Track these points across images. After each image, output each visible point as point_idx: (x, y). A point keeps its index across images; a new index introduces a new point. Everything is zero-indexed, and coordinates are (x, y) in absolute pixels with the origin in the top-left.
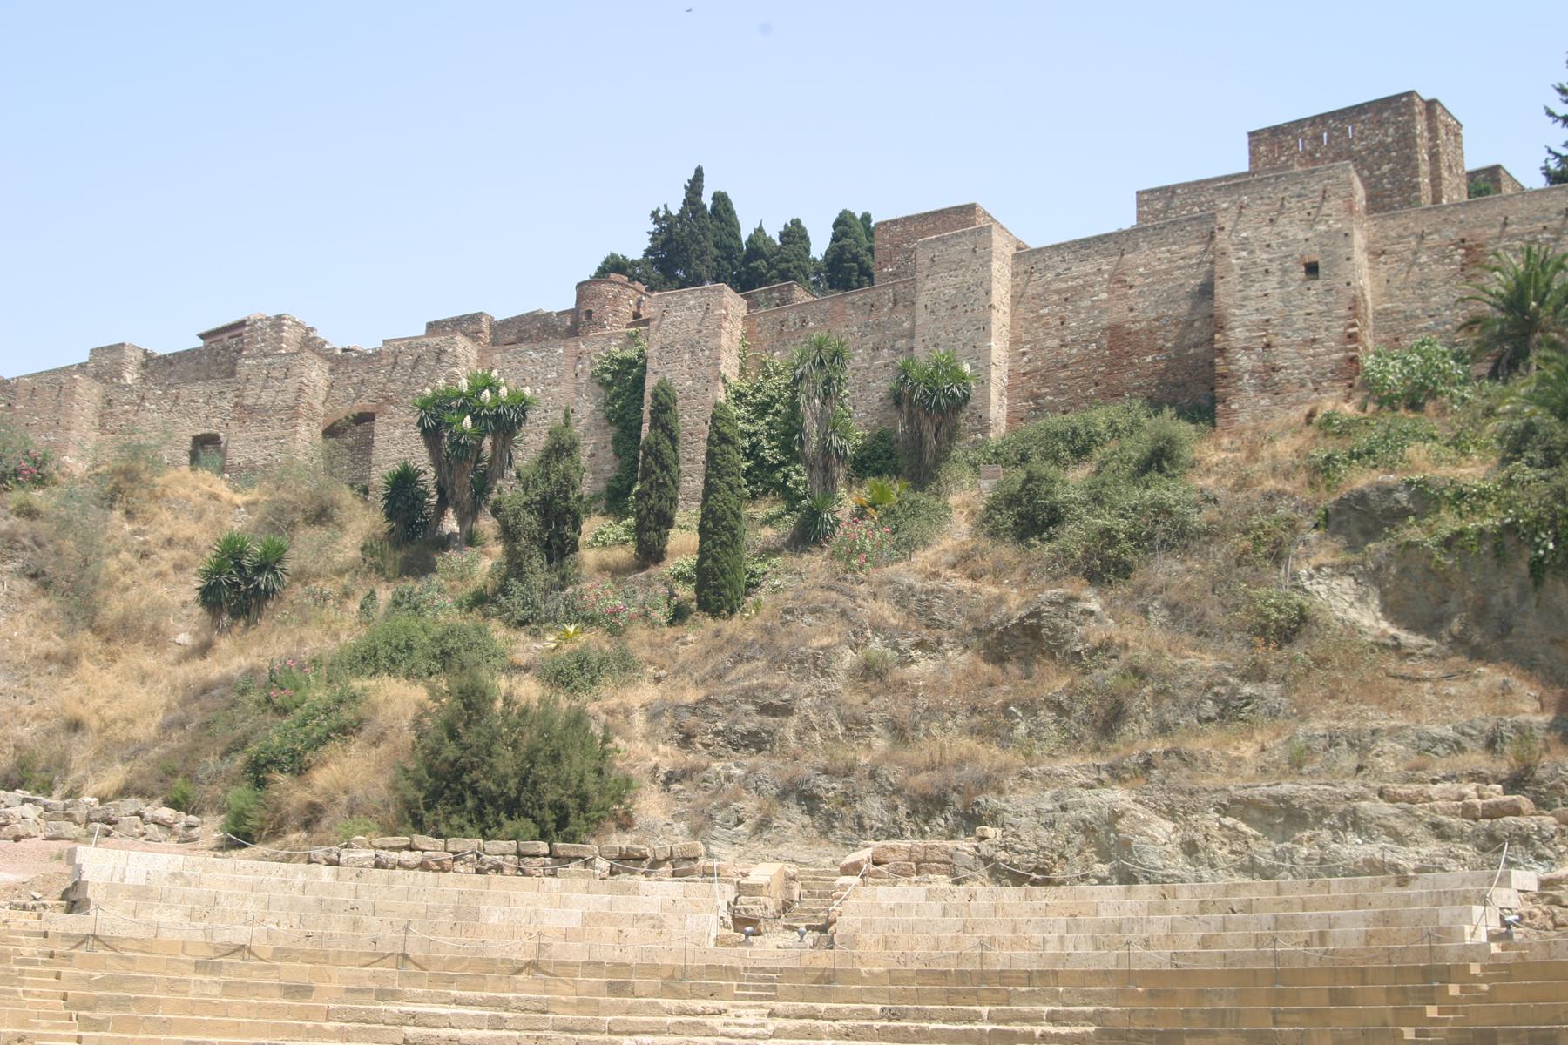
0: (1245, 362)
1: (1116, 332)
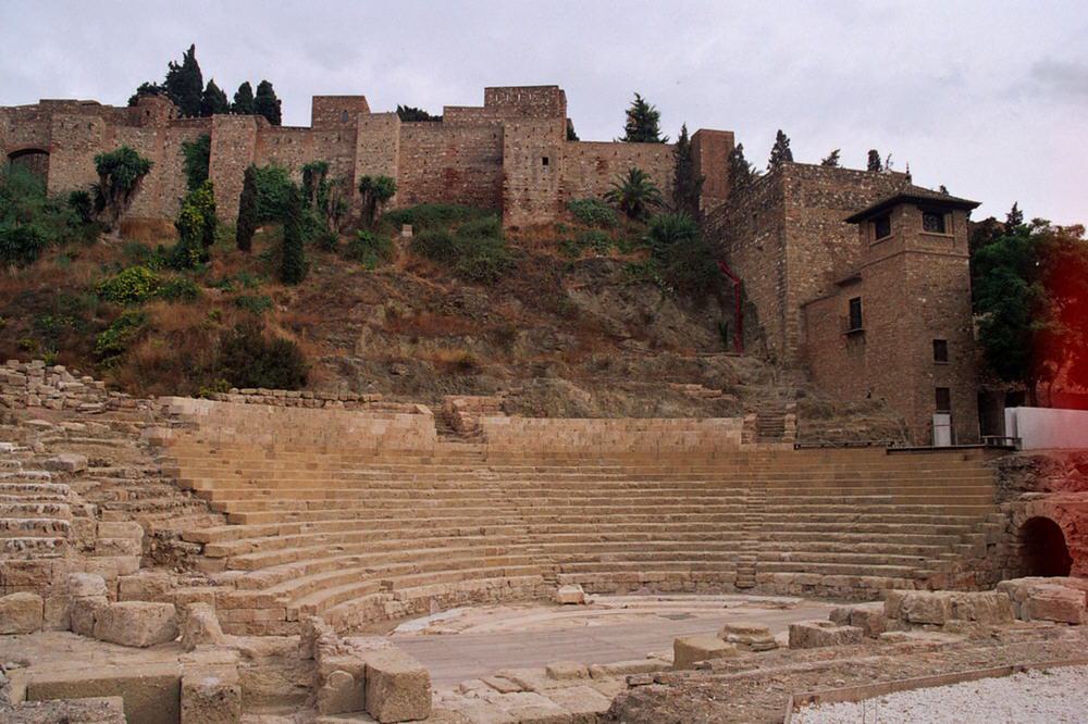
0: (516, 195)
1: (451, 174)
